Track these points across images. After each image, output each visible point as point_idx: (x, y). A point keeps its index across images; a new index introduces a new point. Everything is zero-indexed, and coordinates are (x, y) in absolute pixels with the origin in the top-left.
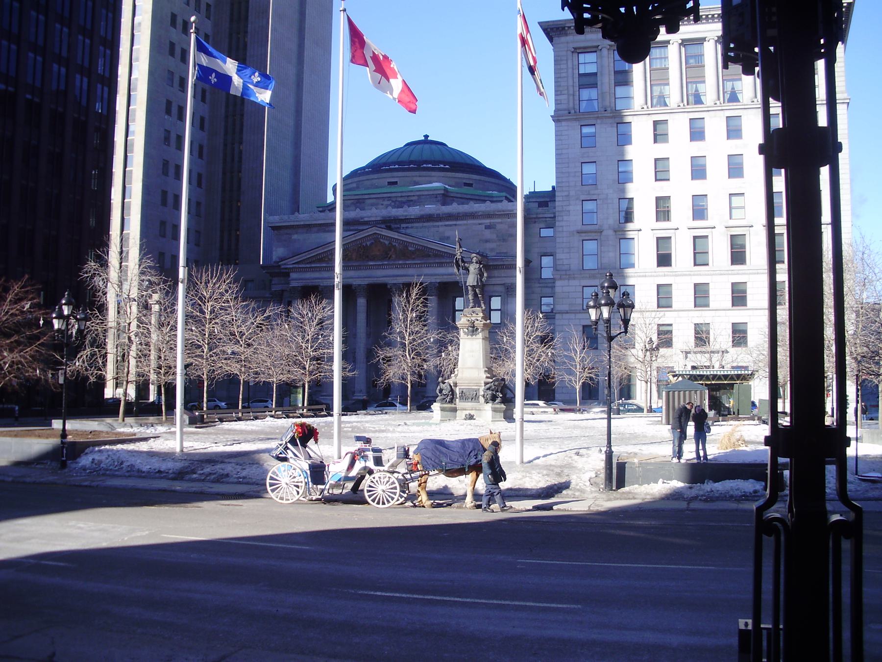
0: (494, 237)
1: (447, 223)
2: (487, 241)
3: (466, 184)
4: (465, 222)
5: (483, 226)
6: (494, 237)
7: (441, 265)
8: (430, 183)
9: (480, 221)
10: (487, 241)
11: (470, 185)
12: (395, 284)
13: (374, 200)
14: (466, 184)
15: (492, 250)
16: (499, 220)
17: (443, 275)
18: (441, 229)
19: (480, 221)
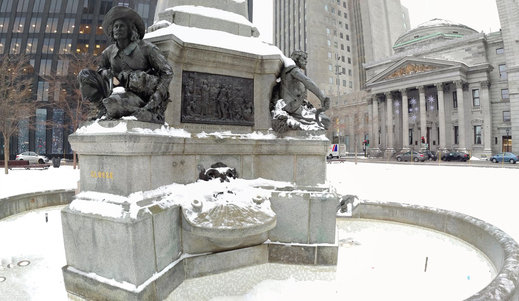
0: (471, 55)
1: (446, 51)
2: (467, 58)
3: (454, 32)
4: (454, 49)
5: (464, 50)
6: (471, 55)
7: (442, 72)
8: (435, 33)
9: (463, 48)
10: (467, 58)
11: (457, 33)
12: (420, 86)
13: (409, 47)
14: (454, 32)
15: (471, 63)
16: (472, 45)
17: (444, 78)
18: (443, 56)
19: (463, 48)
